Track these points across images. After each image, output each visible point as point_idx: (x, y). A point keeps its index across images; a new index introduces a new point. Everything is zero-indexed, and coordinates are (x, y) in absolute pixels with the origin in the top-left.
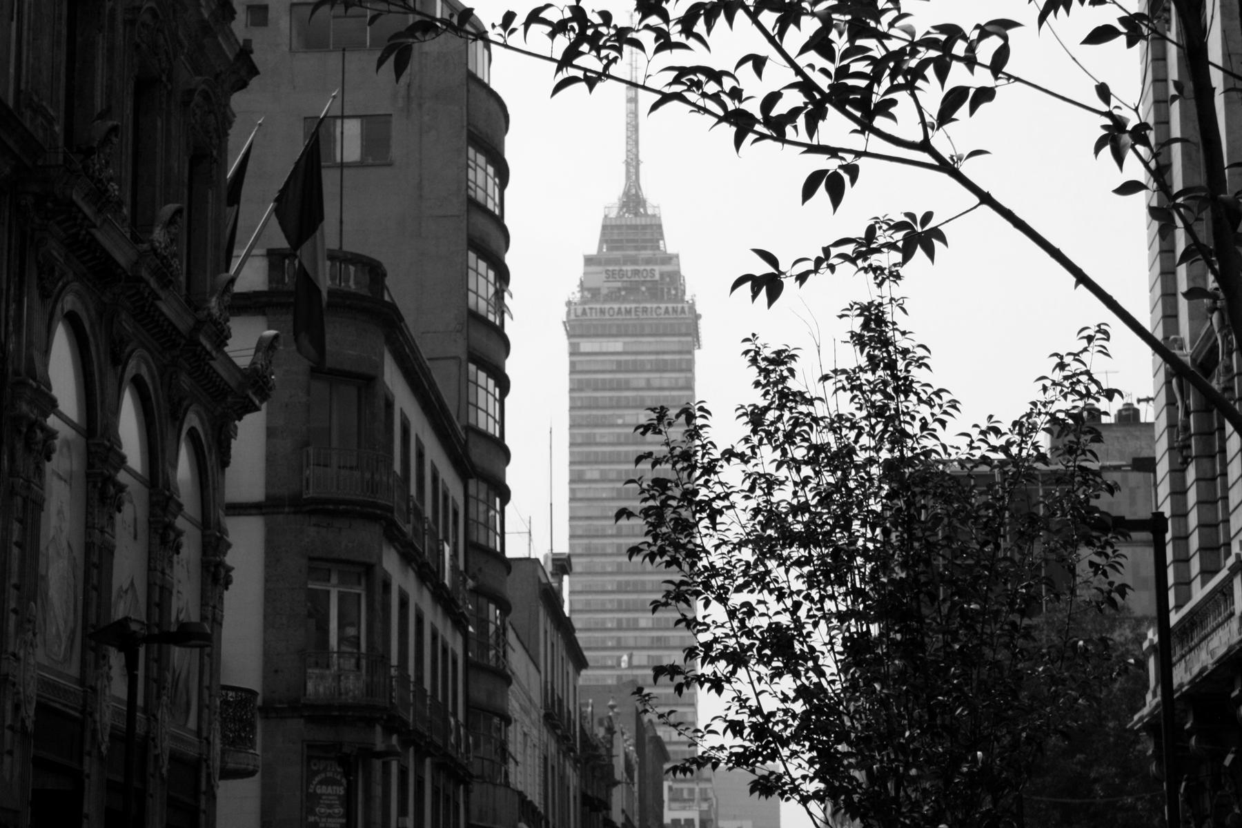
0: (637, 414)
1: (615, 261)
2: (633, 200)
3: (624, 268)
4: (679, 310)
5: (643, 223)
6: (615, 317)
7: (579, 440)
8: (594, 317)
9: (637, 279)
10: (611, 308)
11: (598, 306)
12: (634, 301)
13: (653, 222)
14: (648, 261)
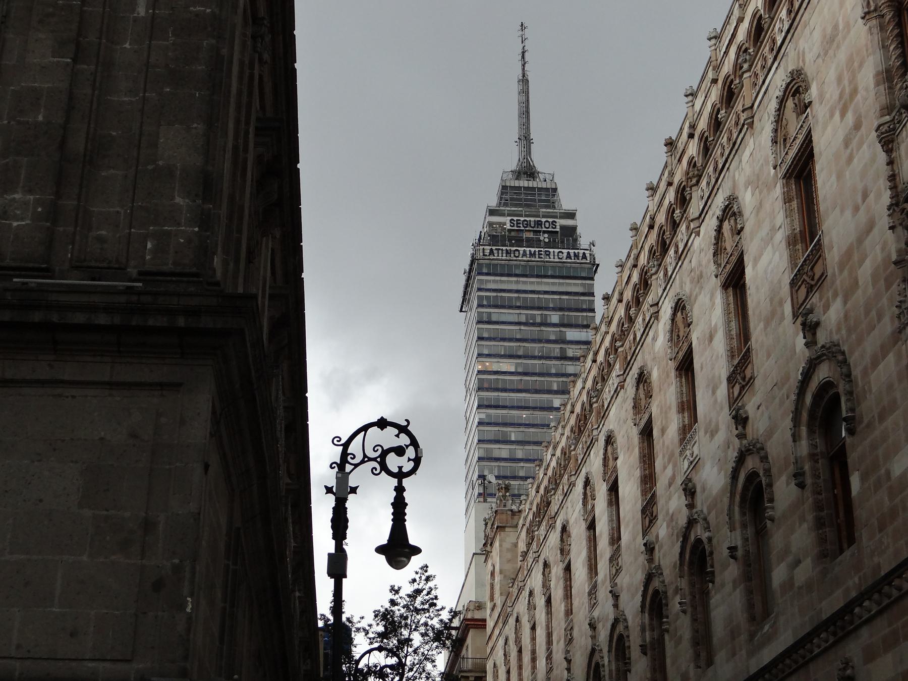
4: (581, 255)
11: (504, 248)
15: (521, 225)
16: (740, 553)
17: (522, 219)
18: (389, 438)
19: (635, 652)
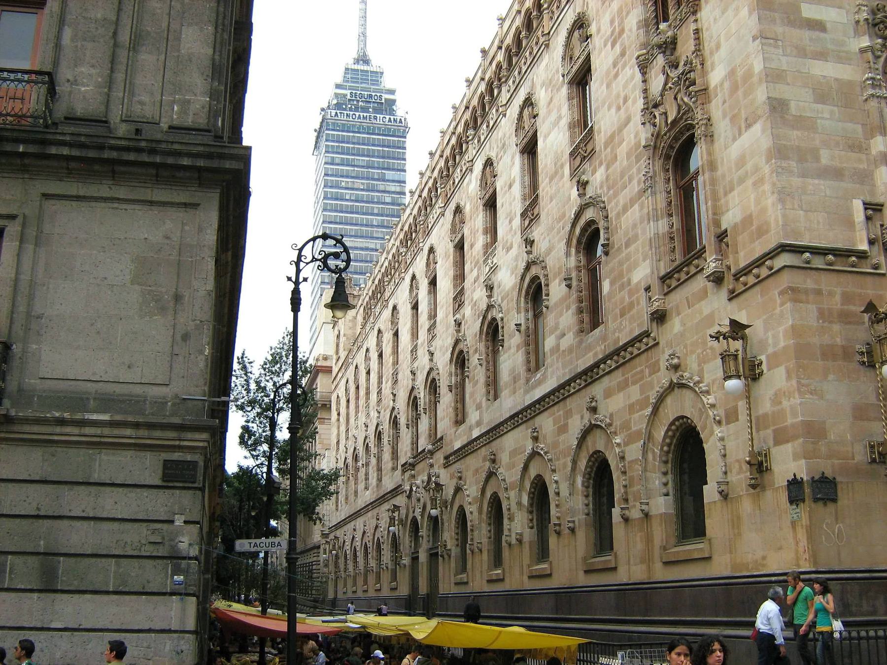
6: (356, 120)
11: (345, 112)
16: (523, 328)
17: (359, 92)
18: (330, 246)
19: (443, 390)
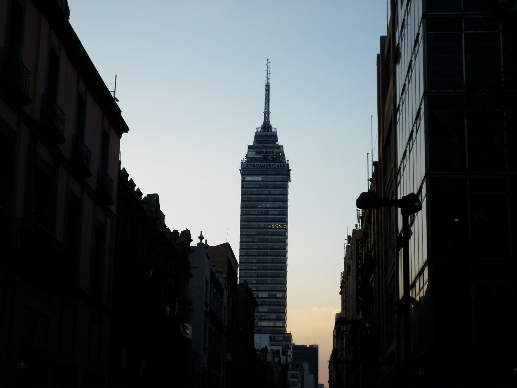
0: (266, 204)
1: (259, 148)
2: (266, 126)
3: (263, 150)
4: (283, 165)
5: (270, 134)
6: (259, 168)
7: (244, 213)
8: (251, 168)
9: (267, 154)
10: (257, 165)
11: (253, 164)
12: (266, 162)
13: (274, 134)
14: (271, 148)
15: (260, 153)
